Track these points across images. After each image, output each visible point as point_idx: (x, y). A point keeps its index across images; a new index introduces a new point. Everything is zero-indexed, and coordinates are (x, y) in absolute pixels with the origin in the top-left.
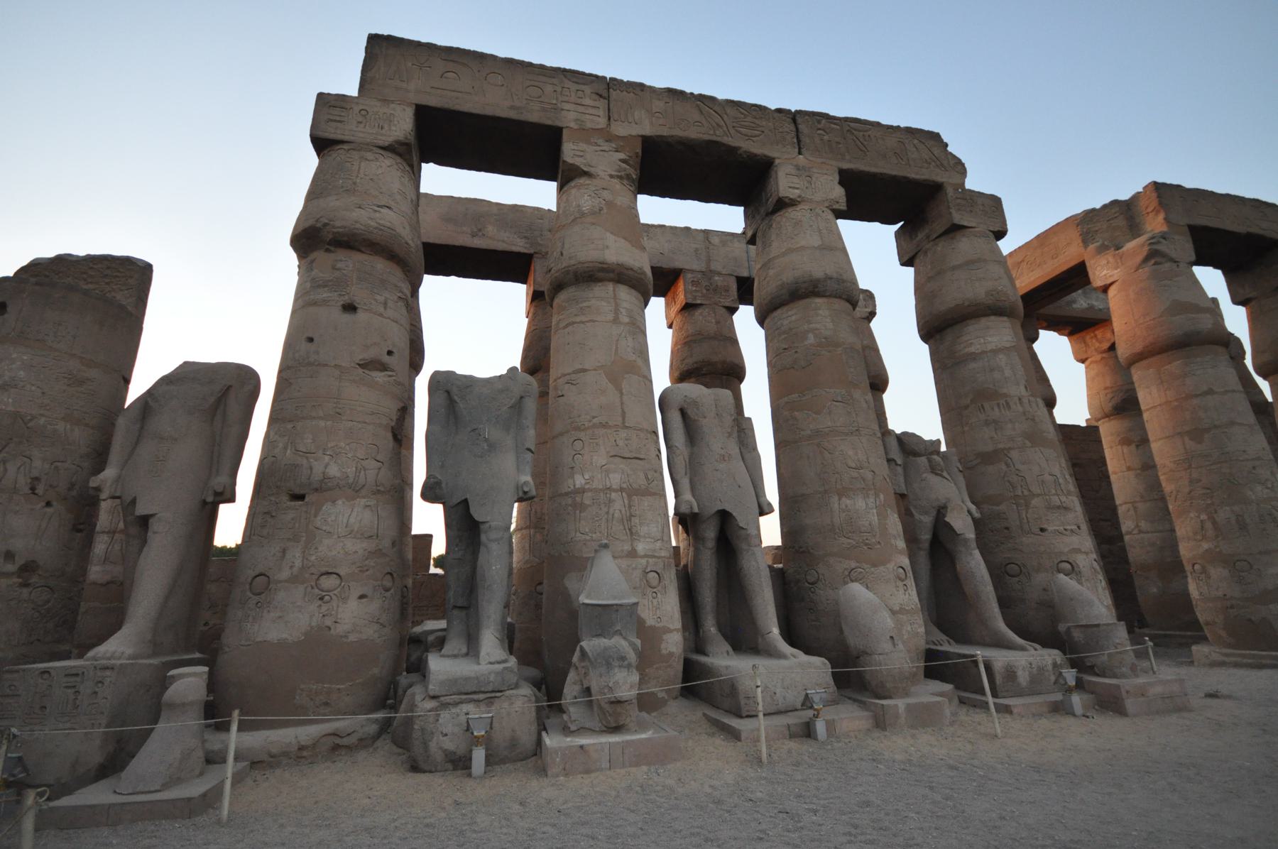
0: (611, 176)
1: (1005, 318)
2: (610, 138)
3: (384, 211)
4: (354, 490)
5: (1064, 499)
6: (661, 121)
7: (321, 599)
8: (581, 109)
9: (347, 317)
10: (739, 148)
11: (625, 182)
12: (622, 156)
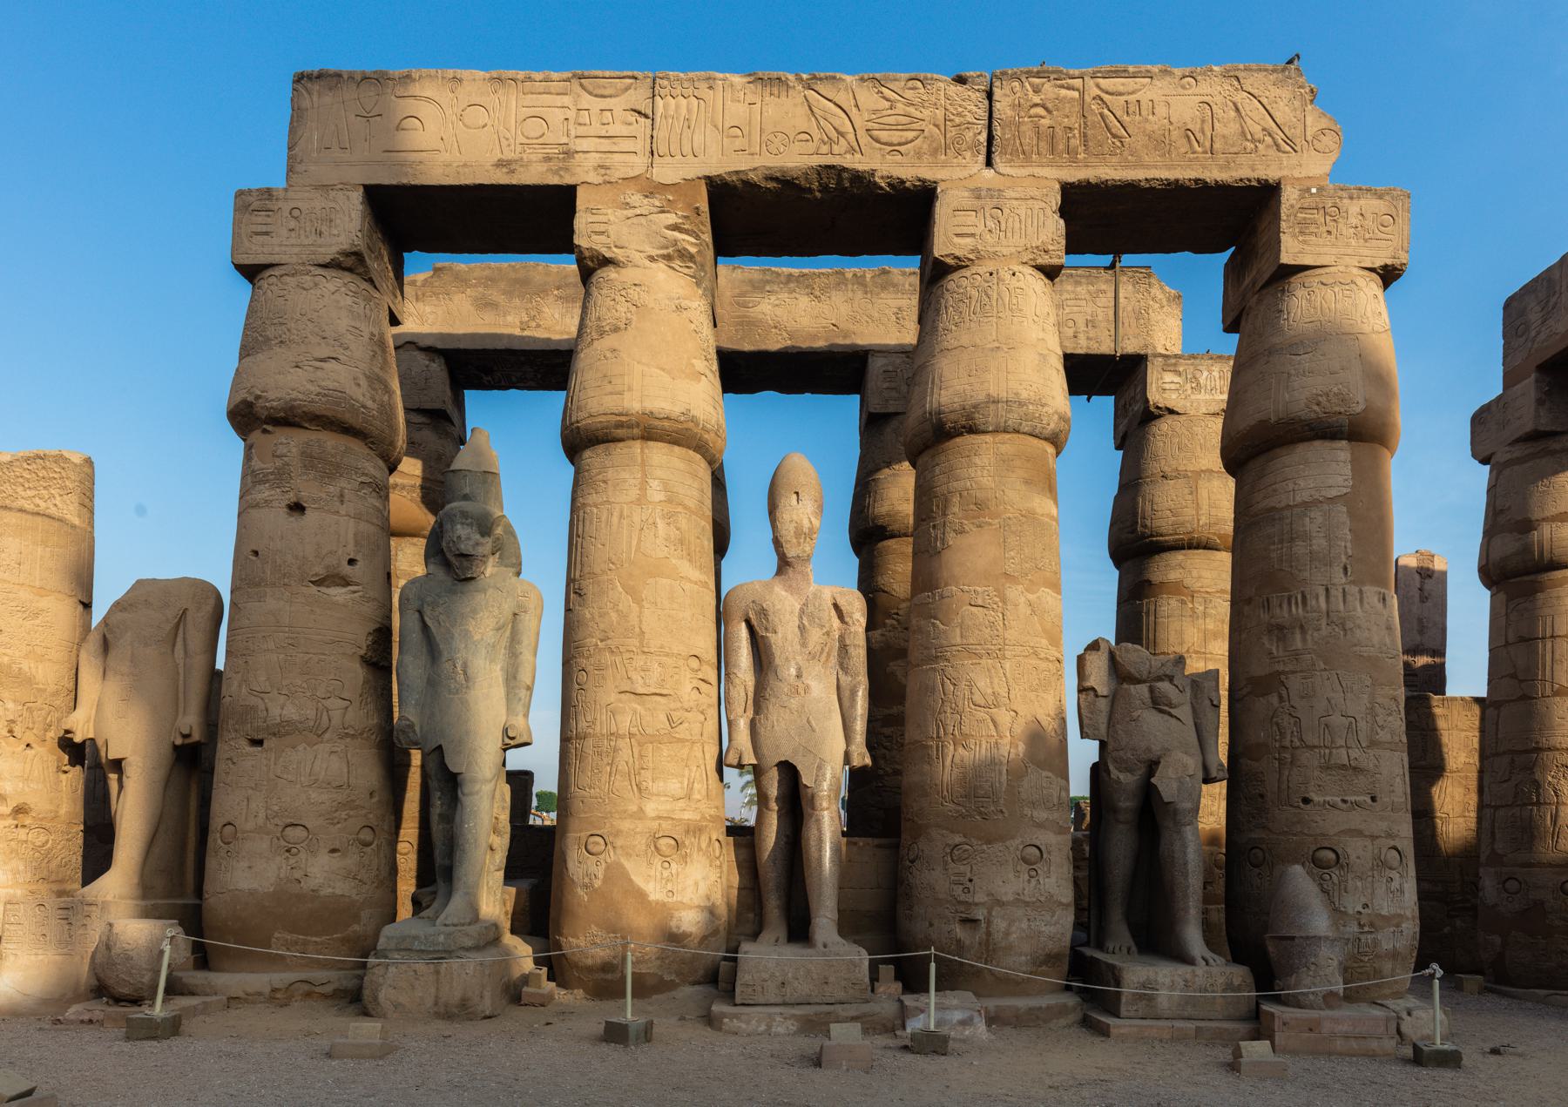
0: (652, 259)
1: (1344, 443)
2: (652, 189)
3: (331, 365)
4: (317, 732)
5: (1355, 753)
6: (738, 144)
7: (288, 851)
8: (606, 145)
9: (294, 522)
10: (873, 173)
11: (677, 263)
12: (671, 219)
